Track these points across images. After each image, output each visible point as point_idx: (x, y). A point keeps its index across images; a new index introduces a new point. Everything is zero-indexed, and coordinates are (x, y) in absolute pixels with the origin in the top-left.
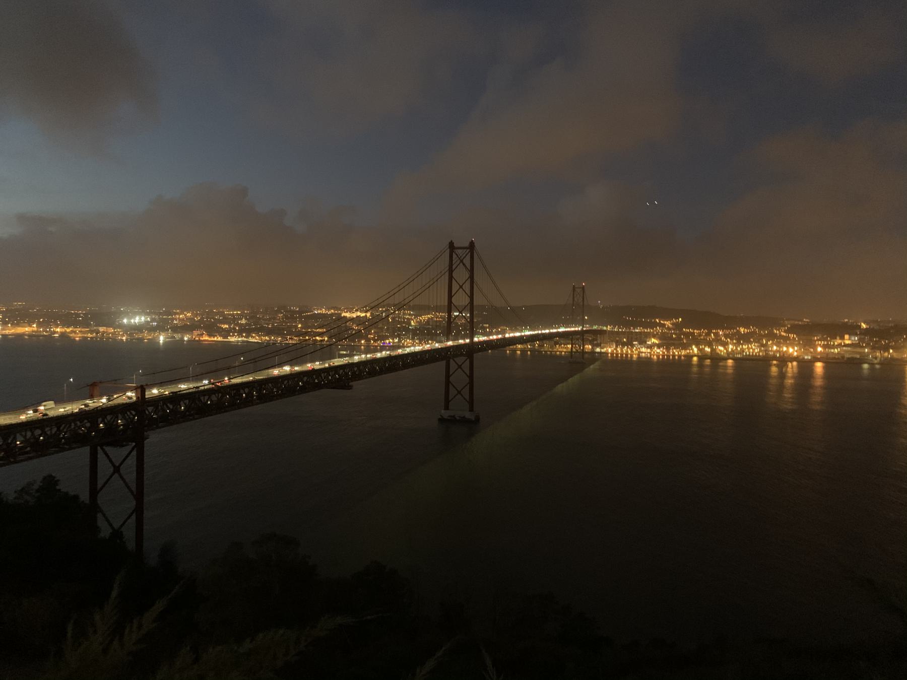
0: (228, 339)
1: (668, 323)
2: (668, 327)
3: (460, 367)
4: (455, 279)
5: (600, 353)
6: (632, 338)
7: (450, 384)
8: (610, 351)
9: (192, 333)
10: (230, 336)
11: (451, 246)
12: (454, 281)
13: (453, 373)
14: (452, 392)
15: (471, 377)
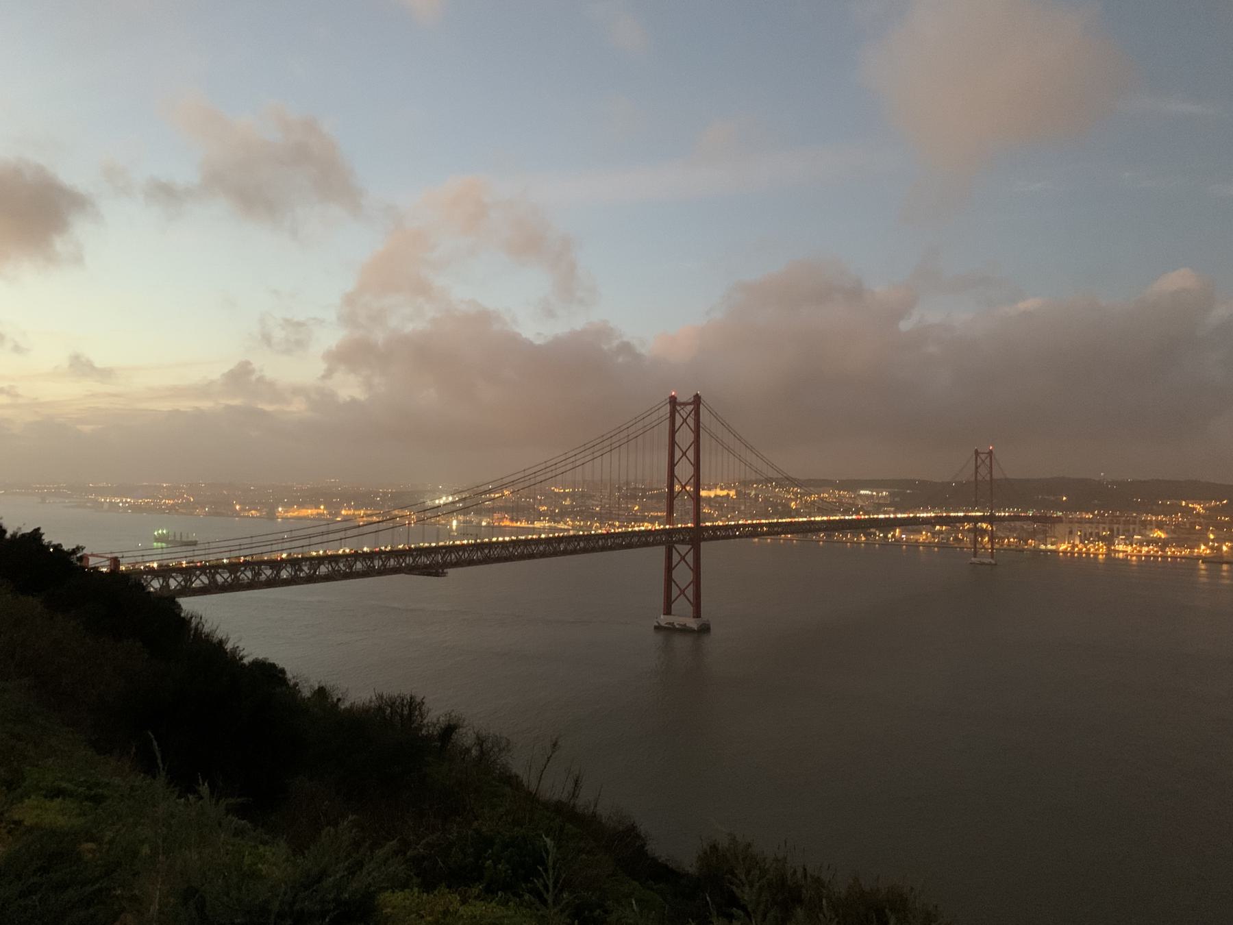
0: (534, 524)
1: (1199, 508)
2: (1198, 513)
3: (683, 558)
4: (678, 446)
5: (1046, 551)
6: (1118, 529)
7: (673, 583)
8: (1063, 547)
9: (493, 516)
10: (544, 520)
11: (673, 401)
12: (677, 448)
13: (677, 565)
14: (675, 592)
15: (697, 570)
